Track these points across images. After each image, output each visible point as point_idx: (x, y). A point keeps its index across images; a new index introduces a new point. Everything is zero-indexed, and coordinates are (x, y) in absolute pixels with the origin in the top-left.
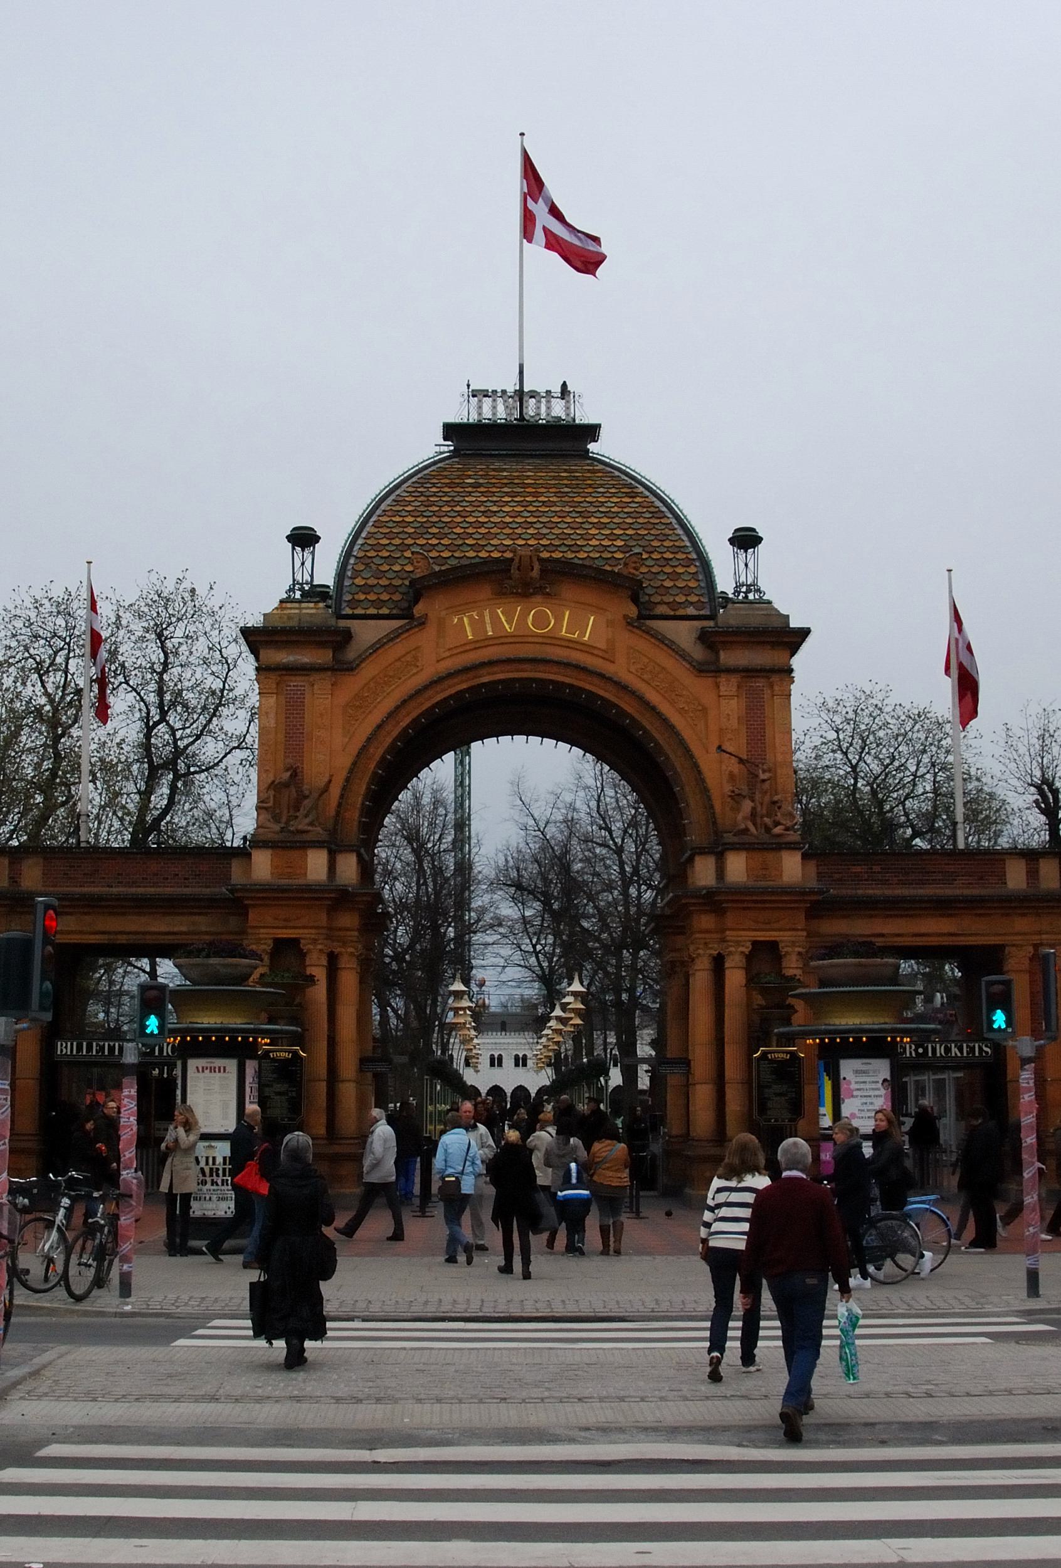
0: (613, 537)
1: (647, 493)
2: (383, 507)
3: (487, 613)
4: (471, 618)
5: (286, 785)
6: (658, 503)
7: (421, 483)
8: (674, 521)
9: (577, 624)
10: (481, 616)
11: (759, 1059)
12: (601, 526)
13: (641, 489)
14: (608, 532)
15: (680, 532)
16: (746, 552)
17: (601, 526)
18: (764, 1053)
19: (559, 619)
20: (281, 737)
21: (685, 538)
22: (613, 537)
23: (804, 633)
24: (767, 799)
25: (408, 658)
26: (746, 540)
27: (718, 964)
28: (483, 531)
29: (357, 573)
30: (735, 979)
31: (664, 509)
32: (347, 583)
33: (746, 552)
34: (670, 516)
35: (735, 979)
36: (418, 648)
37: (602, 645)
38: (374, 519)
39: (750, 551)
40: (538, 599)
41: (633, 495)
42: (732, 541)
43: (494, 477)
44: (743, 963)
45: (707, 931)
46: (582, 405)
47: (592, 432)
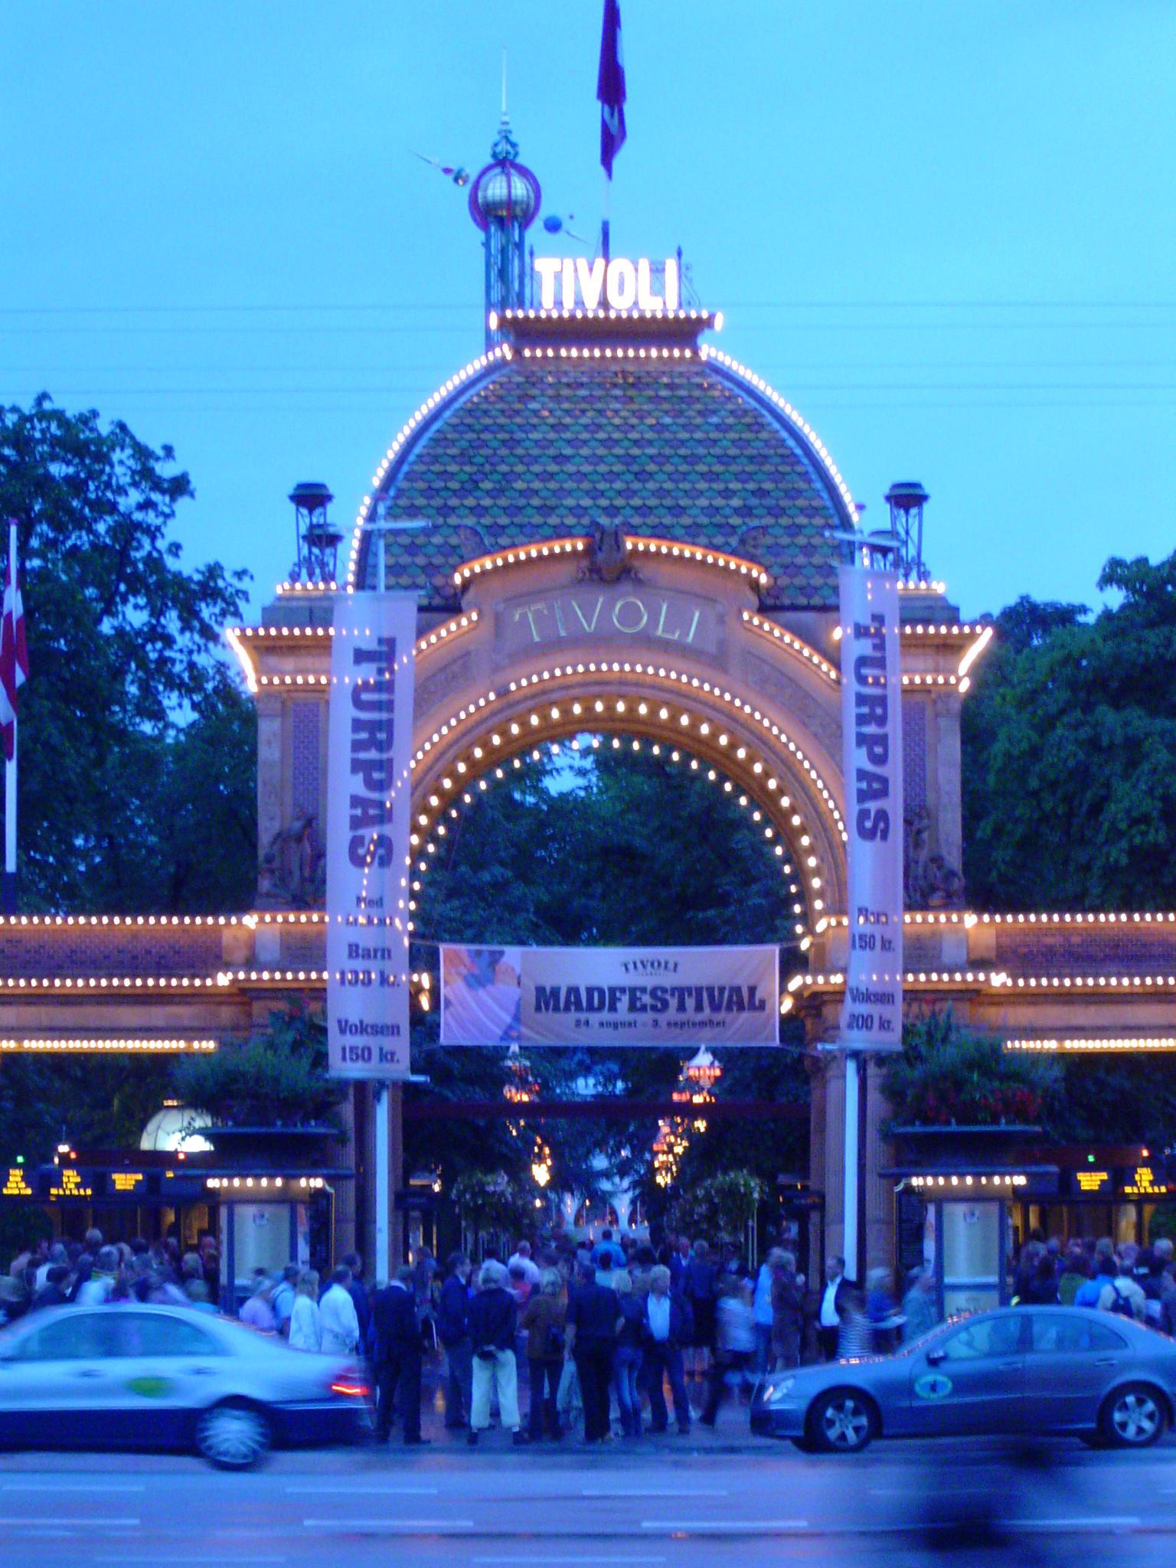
0: (727, 494)
1: (776, 425)
2: (418, 450)
3: (557, 605)
6: (791, 443)
8: (810, 469)
9: (679, 620)
10: (551, 608)
12: (711, 477)
13: (769, 418)
14: (722, 486)
15: (818, 485)
16: (907, 512)
17: (711, 477)
20: (289, 773)
21: (825, 495)
22: (727, 494)
25: (455, 668)
26: (907, 498)
28: (552, 485)
31: (798, 451)
33: (907, 512)
34: (805, 461)
36: (467, 654)
37: (712, 648)
38: (405, 468)
39: (914, 511)
40: (626, 587)
41: (757, 426)
42: (888, 498)
43: (568, 399)
46: (690, 281)
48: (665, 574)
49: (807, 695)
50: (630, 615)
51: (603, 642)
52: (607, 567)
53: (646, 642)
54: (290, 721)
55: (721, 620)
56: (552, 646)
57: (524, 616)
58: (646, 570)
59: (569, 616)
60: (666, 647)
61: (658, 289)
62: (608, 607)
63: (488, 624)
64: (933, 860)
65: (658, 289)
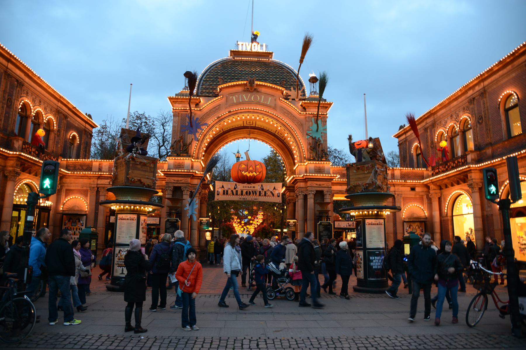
4: (236, 97)
5: (179, 141)
7: (224, 64)
10: (239, 97)
11: (319, 225)
18: (321, 223)
19: (261, 98)
20: (179, 129)
23: (330, 104)
24: (320, 150)
27: (305, 197)
29: (203, 85)
30: (311, 201)
32: (200, 87)
35: (311, 201)
40: (255, 93)
44: (313, 197)
45: (303, 188)
47: (271, 54)
48: (263, 90)
49: (294, 116)
50: (256, 98)
51: (250, 103)
52: (251, 88)
53: (259, 103)
54: (180, 118)
55: (275, 100)
56: (238, 104)
57: (233, 98)
58: (260, 89)
59: (243, 98)
60: (263, 105)
61: (262, 49)
62: (251, 96)
63: (224, 99)
64: (322, 151)
65: (262, 49)
